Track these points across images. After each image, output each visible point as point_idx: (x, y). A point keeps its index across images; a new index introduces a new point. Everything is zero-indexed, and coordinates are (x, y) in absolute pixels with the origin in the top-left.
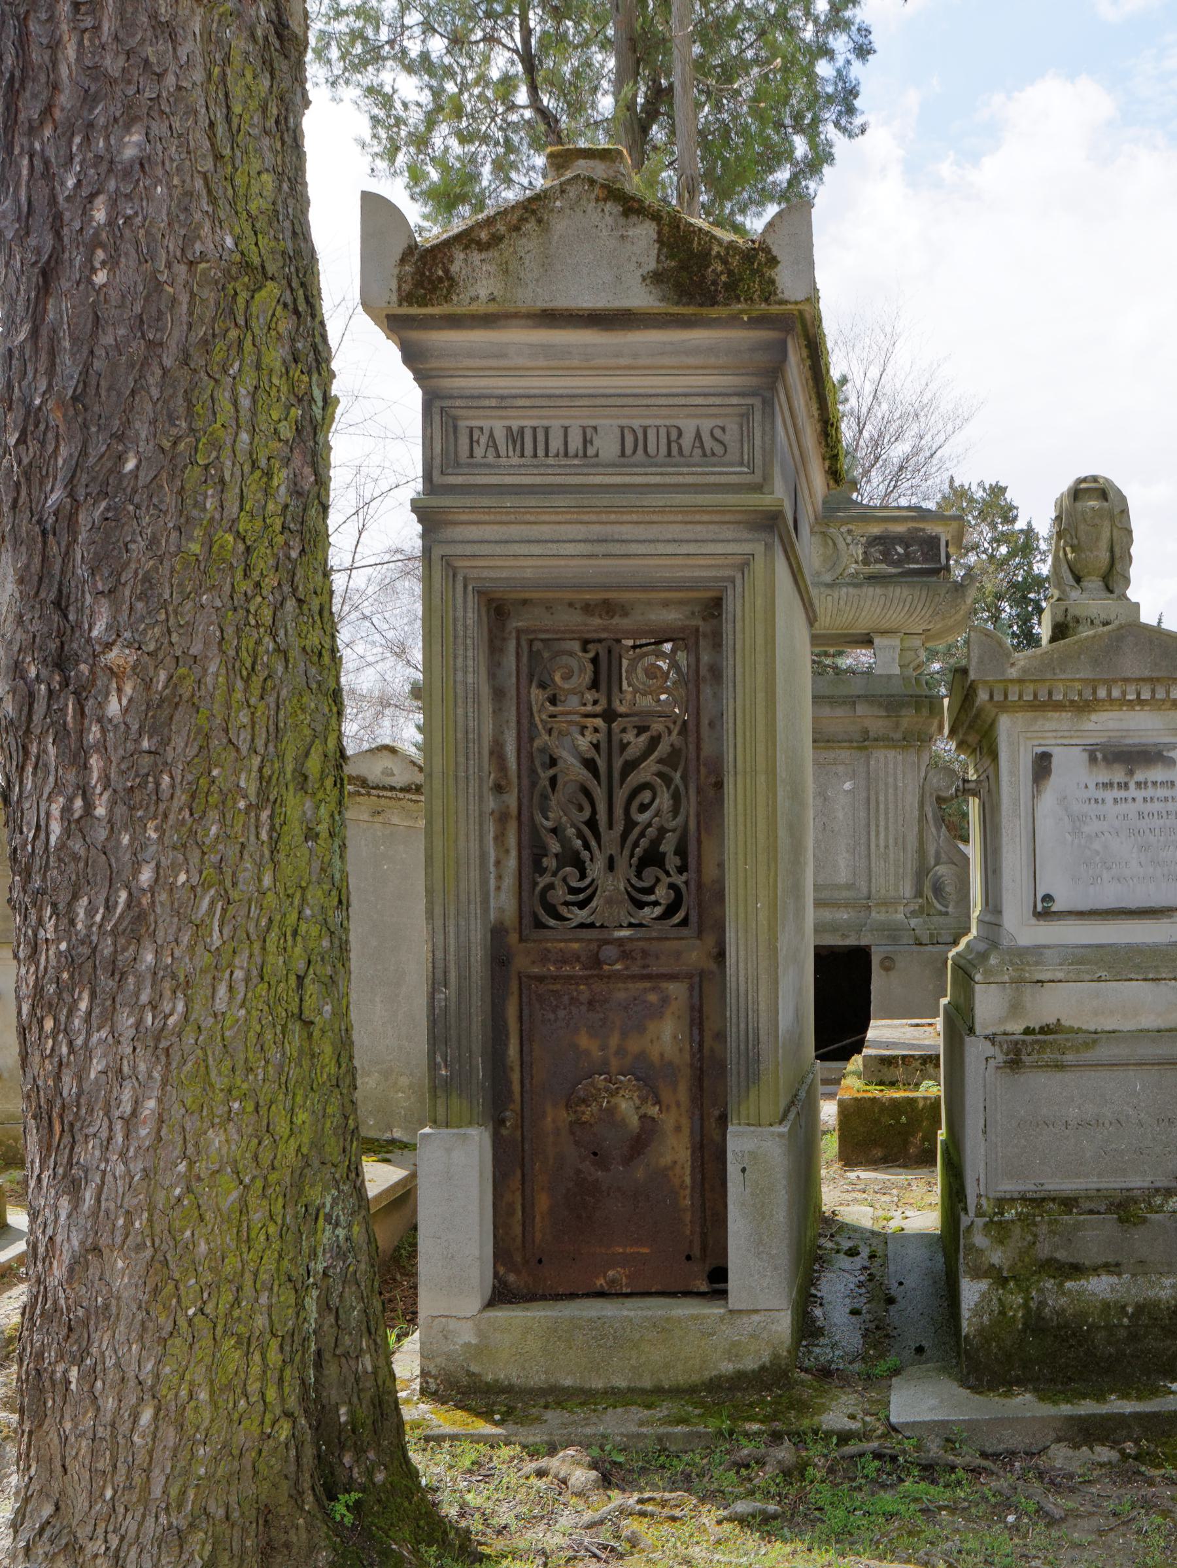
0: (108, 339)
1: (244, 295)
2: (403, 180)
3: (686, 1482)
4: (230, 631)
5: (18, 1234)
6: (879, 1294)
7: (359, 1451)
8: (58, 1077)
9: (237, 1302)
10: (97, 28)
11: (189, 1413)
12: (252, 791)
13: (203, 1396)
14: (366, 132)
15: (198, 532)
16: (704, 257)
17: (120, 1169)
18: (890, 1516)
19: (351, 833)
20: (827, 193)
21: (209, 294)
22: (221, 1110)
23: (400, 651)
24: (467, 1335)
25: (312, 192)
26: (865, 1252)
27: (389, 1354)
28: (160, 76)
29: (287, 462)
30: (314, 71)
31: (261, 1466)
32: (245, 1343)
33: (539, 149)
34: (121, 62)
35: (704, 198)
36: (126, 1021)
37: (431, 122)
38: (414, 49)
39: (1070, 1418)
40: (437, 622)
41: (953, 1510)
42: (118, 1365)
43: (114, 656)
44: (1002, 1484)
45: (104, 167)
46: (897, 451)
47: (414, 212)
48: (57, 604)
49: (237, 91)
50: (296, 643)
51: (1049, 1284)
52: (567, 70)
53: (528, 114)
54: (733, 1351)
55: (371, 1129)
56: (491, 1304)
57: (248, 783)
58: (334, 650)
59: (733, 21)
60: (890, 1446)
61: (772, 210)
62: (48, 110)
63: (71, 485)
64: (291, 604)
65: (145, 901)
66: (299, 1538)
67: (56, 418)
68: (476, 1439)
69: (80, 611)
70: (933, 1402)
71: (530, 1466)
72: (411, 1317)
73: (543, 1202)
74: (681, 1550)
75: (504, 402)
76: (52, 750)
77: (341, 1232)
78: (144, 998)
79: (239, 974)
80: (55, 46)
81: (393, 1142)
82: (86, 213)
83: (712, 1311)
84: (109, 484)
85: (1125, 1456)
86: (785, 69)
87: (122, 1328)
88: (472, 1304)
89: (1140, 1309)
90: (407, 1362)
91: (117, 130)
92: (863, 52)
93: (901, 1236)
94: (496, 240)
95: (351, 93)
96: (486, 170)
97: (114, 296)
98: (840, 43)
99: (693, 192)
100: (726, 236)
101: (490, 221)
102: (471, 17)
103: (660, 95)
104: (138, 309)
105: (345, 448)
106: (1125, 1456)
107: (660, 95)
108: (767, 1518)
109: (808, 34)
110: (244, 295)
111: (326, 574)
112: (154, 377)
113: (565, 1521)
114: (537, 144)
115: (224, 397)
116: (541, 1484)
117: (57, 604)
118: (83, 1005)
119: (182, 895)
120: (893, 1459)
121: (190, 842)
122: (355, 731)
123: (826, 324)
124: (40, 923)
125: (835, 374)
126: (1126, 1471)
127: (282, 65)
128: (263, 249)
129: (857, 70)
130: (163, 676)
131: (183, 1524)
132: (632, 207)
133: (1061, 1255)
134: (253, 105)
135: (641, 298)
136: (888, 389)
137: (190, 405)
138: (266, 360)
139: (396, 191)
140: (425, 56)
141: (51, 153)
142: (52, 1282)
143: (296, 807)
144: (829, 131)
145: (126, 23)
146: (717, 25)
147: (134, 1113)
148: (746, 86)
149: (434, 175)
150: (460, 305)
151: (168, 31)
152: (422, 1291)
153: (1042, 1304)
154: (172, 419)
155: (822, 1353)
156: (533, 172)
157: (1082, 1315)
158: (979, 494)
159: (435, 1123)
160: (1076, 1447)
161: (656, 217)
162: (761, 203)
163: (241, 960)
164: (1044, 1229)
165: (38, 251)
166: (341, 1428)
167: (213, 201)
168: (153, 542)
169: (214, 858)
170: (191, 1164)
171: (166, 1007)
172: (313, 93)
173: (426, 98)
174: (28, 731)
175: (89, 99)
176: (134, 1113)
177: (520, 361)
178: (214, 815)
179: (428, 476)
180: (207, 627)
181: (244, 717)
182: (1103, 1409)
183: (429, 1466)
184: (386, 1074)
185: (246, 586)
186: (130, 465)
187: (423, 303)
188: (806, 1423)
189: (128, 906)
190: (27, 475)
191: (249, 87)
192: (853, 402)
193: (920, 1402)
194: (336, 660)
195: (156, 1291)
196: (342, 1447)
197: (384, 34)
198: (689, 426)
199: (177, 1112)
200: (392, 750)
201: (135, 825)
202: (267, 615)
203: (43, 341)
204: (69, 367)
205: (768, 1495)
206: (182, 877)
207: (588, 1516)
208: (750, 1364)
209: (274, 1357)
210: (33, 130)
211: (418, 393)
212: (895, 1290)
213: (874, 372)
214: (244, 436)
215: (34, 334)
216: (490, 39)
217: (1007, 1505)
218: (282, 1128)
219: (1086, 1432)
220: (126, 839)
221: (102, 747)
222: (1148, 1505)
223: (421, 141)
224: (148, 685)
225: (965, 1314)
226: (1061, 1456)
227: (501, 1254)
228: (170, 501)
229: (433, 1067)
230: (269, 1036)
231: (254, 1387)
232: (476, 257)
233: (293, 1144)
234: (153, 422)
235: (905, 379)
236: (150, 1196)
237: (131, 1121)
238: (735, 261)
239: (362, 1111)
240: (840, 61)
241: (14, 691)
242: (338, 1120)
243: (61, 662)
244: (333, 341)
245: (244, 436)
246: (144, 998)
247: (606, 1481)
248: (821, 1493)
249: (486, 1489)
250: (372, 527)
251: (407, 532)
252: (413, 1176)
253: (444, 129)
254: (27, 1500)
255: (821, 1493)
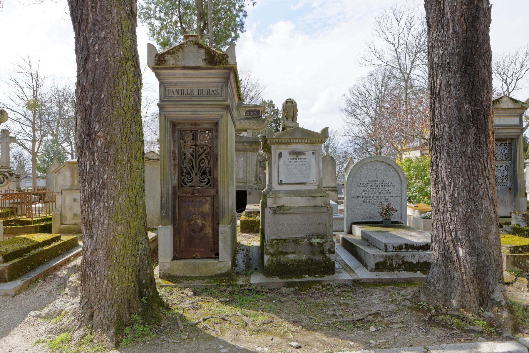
0: (98, 72)
1: (125, 63)
2: (156, 41)
3: (211, 295)
4: (122, 129)
5: (81, 246)
6: (248, 258)
7: (147, 289)
8: (88, 216)
9: (123, 259)
10: (96, 11)
11: (114, 281)
12: (126, 160)
13: (117, 278)
14: (148, 32)
15: (116, 110)
16: (214, 56)
17: (101, 234)
18: (250, 301)
19: (145, 168)
20: (238, 44)
21: (118, 63)
22: (120, 222)
23: (155, 133)
24: (168, 266)
25: (138, 43)
26: (246, 250)
27: (153, 270)
28: (108, 21)
29: (133, 96)
30: (138, 20)
31: (128, 292)
32: (125, 268)
33: (182, 35)
34: (101, 18)
35: (214, 44)
36: (102, 205)
37: (161, 30)
38: (158, 16)
39: (285, 282)
40: (162, 127)
41: (263, 300)
42: (100, 272)
43: (99, 134)
44: (272, 295)
45: (97, 38)
46: (252, 94)
47: (158, 47)
48: (88, 124)
49: (123, 24)
50: (135, 131)
51: (281, 256)
52: (187, 19)
53: (180, 28)
54: (220, 269)
55: (149, 226)
56: (173, 260)
57: (126, 158)
58: (142, 133)
59: (220, 10)
60: (250, 288)
61: (227, 47)
62: (86, 27)
63: (91, 100)
64: (134, 124)
65: (105, 181)
66: (135, 306)
67: (88, 87)
68: (170, 286)
69: (93, 125)
70: (259, 279)
71: (180, 292)
72: (157, 263)
73: (183, 240)
74: (210, 308)
75: (175, 84)
76: (87, 152)
77: (144, 246)
78: (105, 200)
79: (124, 196)
80: (88, 15)
81: (154, 228)
82: (94, 47)
83: (216, 261)
84: (99, 100)
85: (296, 290)
86: (230, 19)
87: (101, 265)
88: (169, 260)
89: (299, 261)
90: (156, 271)
91: (100, 31)
92: (245, 16)
93: (253, 247)
94: (174, 53)
95: (145, 24)
96: (172, 39)
97: (99, 64)
98: (241, 14)
99: (212, 43)
100: (219, 52)
101: (172, 49)
102: (169, 9)
103: (206, 24)
104: (104, 66)
105: (145, 93)
106: (296, 290)
107: (206, 24)
108: (227, 302)
109: (235, 12)
110: (125, 63)
111: (141, 118)
112: (107, 80)
113: (187, 302)
114: (182, 34)
115: (121, 83)
116: (182, 295)
117: (88, 124)
118: (93, 202)
119: (112, 180)
120: (251, 290)
121: (114, 170)
122: (146, 148)
123: (238, 69)
124: (85, 186)
125: (240, 79)
126: (296, 293)
127: (132, 19)
128: (129, 54)
129: (244, 20)
130: (109, 138)
131: (113, 303)
132: (200, 46)
133: (284, 250)
134: (126, 26)
135: (202, 64)
136: (250, 82)
137: (114, 85)
138: (129, 76)
139: (154, 43)
140: (160, 17)
141: (87, 36)
142: (87, 256)
143: (135, 163)
144: (239, 31)
145: (102, 10)
146: (217, 11)
147: (103, 223)
148: (222, 23)
149: (162, 40)
150: (167, 65)
151: (110, 12)
152: (159, 257)
153: (280, 260)
154: (111, 88)
155: (237, 269)
156: (181, 39)
157: (288, 262)
158: (268, 102)
159: (162, 225)
160: (287, 288)
161: (205, 48)
162: (225, 46)
163: (124, 193)
164: (280, 245)
165: (84, 55)
166: (144, 284)
167: (119, 45)
168: (107, 111)
169: (119, 173)
170: (114, 233)
171: (110, 202)
172: (138, 24)
173: (160, 25)
174: (83, 148)
175: (94, 25)
176: (103, 223)
177: (178, 76)
178: (119, 165)
179: (160, 99)
180: (117, 128)
181: (125, 146)
182: (292, 280)
183: (161, 292)
184: (152, 215)
185: (125, 120)
186: (102, 97)
187: (160, 65)
188: (234, 283)
189: (102, 182)
190: (82, 98)
191: (126, 23)
192: (243, 84)
193: (256, 279)
194: (143, 135)
195: (108, 257)
196: (144, 288)
197: (152, 13)
198: (211, 89)
199: (112, 223)
200: (153, 152)
201: (104, 167)
202: (129, 125)
203: (86, 72)
204: (91, 77)
205: (227, 297)
206: (113, 177)
207: (192, 301)
208: (223, 272)
209: (130, 270)
210: (84, 31)
211: (158, 83)
212: (251, 257)
213: (247, 78)
214: (125, 91)
215: (84, 71)
216: (173, 13)
217: (273, 299)
218: (132, 226)
219: (289, 285)
220: (102, 169)
221: (97, 151)
222: (301, 299)
223: (159, 33)
224: (106, 139)
225: (265, 262)
226: (284, 290)
227: (175, 250)
228: (110, 103)
229: (161, 214)
230: (129, 208)
231: (127, 276)
232: (170, 56)
233: (134, 229)
234: (107, 88)
235: (253, 80)
236: (106, 239)
237: (103, 224)
238: (220, 57)
239: (148, 222)
240: (241, 18)
241: (80, 140)
242: (143, 224)
243: (89, 135)
244: (142, 72)
245: (125, 91)
246: (105, 200)
247: (195, 294)
248: (237, 297)
249: (172, 296)
250: (150, 108)
251: (157, 110)
252: (158, 235)
253: (164, 31)
254: (82, 298)
255: (237, 297)
